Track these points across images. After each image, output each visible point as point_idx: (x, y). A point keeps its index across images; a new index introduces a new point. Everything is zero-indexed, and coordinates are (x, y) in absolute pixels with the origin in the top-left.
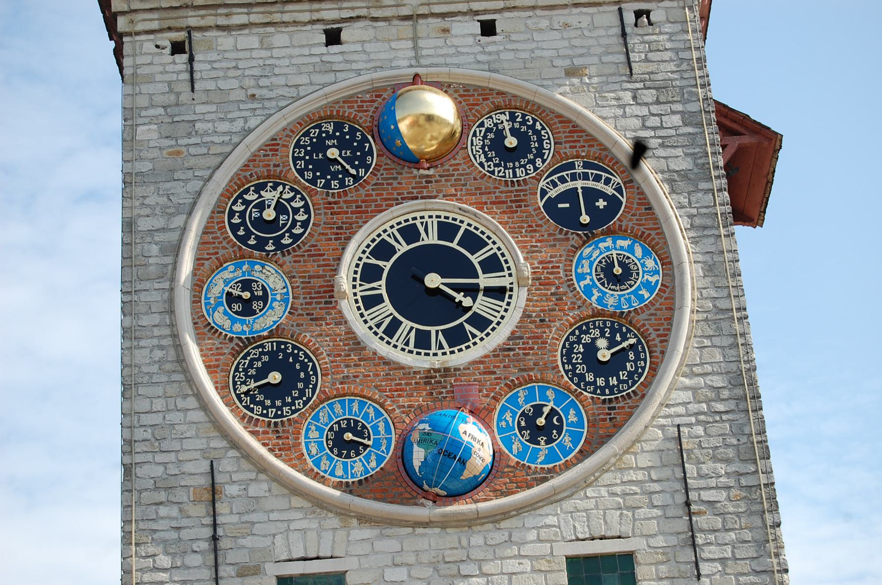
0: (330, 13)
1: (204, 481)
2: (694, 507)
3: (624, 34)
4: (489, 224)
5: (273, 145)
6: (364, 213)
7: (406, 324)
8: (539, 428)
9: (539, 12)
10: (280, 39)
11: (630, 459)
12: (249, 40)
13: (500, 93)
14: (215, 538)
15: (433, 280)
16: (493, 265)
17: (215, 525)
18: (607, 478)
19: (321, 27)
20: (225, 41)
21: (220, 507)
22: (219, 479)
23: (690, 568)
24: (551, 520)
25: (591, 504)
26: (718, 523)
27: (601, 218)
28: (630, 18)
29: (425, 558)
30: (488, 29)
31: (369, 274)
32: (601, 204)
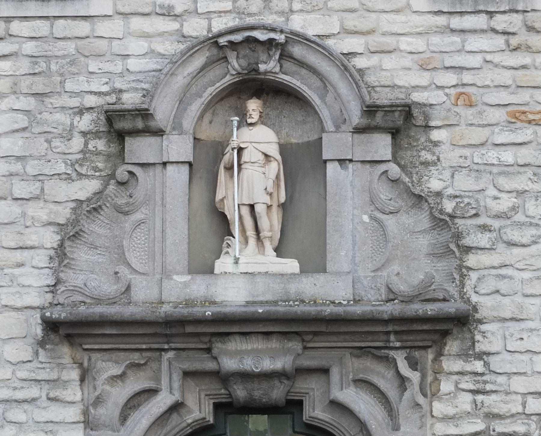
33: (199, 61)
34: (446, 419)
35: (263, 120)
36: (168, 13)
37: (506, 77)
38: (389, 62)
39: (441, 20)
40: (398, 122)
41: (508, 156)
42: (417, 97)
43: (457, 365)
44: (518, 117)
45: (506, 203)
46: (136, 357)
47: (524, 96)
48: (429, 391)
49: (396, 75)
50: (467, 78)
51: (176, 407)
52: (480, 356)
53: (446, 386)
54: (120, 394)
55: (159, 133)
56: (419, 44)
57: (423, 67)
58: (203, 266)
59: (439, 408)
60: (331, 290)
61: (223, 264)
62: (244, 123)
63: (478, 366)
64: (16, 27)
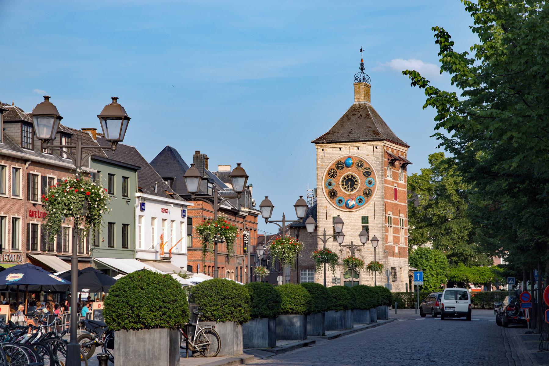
0: (340, 146)
4: (356, 176)
5: (333, 164)
6: (343, 174)
8: (360, 201)
10: (334, 149)
12: (331, 149)
15: (350, 183)
20: (328, 149)
27: (369, 175)
30: (358, 148)
31: (343, 181)
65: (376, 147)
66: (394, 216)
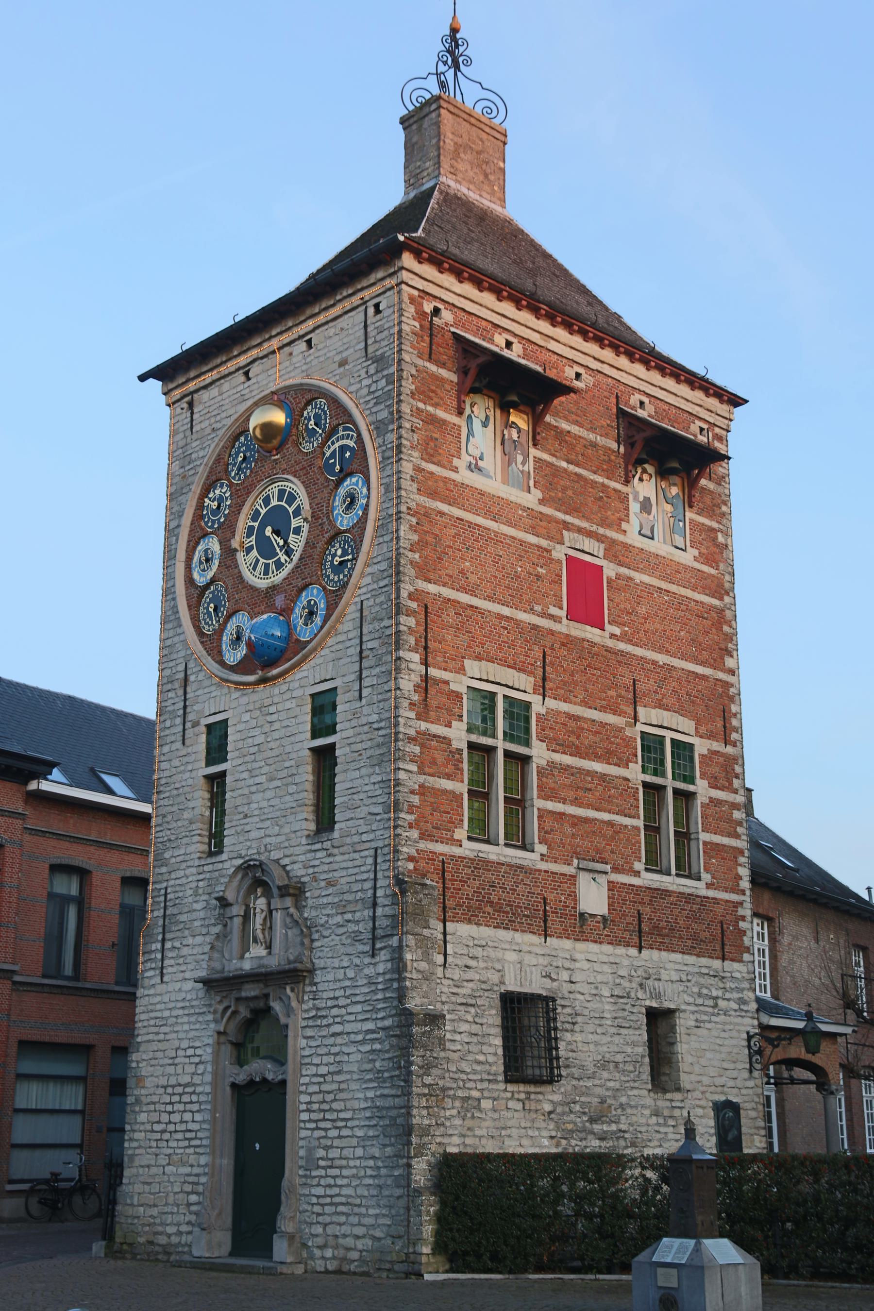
0: (242, 360)
1: (182, 675)
2: (364, 655)
3: (366, 327)
7: (262, 560)
9: (331, 324)
10: (226, 385)
11: (340, 627)
12: (214, 391)
13: (310, 391)
14: (185, 707)
16: (297, 512)
17: (185, 700)
18: (330, 641)
19: (241, 372)
20: (205, 395)
21: (189, 689)
22: (189, 673)
23: (357, 694)
24: (305, 674)
25: (321, 660)
26: (372, 663)
28: (371, 311)
29: (257, 705)
32: (348, 455)
33: (239, 876)
34: (306, 1011)
35: (263, 895)
36: (241, 857)
37: (326, 868)
38: (296, 866)
39: (309, 847)
40: (295, 891)
41: (325, 900)
42: (303, 880)
43: (308, 989)
44: (330, 884)
45: (325, 919)
46: (224, 994)
47: (331, 875)
48: (301, 1001)
49: (297, 870)
50: (316, 870)
51: (235, 1013)
52: (316, 984)
53: (306, 998)
54: (221, 1008)
55: (231, 905)
56: (302, 858)
57: (305, 867)
58: (242, 957)
59: (304, 1007)
60: (273, 963)
61: (247, 955)
62: (256, 898)
63: (314, 988)
64: (206, 868)
65: (377, 311)
66: (551, 703)
